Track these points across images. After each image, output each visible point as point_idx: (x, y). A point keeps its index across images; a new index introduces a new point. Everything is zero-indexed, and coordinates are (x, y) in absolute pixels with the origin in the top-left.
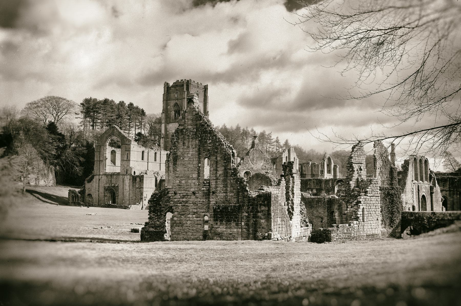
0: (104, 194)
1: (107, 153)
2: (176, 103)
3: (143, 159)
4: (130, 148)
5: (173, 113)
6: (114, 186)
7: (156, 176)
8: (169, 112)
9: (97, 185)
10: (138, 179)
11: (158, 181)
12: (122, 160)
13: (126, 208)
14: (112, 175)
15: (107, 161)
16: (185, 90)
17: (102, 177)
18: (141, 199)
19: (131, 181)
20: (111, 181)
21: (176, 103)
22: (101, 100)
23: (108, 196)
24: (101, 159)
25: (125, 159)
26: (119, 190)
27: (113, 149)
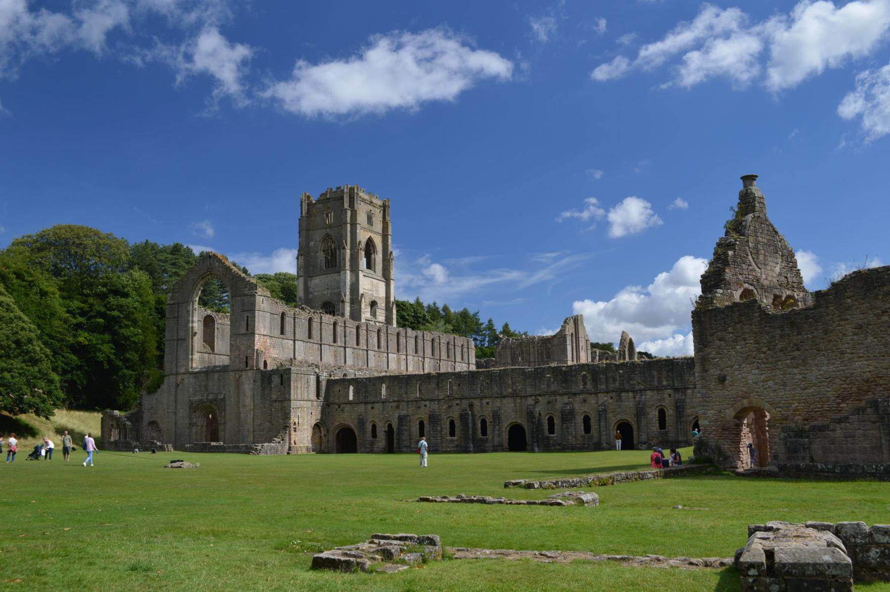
0: (191, 419)
1: (196, 319)
2: (328, 235)
3: (282, 333)
4: (253, 304)
5: (321, 256)
6: (215, 400)
7: (317, 370)
8: (312, 254)
9: (172, 398)
10: (276, 380)
11: (324, 384)
12: (234, 335)
13: (248, 451)
14: (208, 372)
15: (195, 338)
16: (346, 205)
17: (183, 380)
18: (286, 427)
19: (259, 383)
20: (206, 387)
21: (328, 235)
22: (166, 245)
23: (199, 423)
24: (182, 334)
25: (243, 331)
26: (227, 408)
27: (209, 312)
